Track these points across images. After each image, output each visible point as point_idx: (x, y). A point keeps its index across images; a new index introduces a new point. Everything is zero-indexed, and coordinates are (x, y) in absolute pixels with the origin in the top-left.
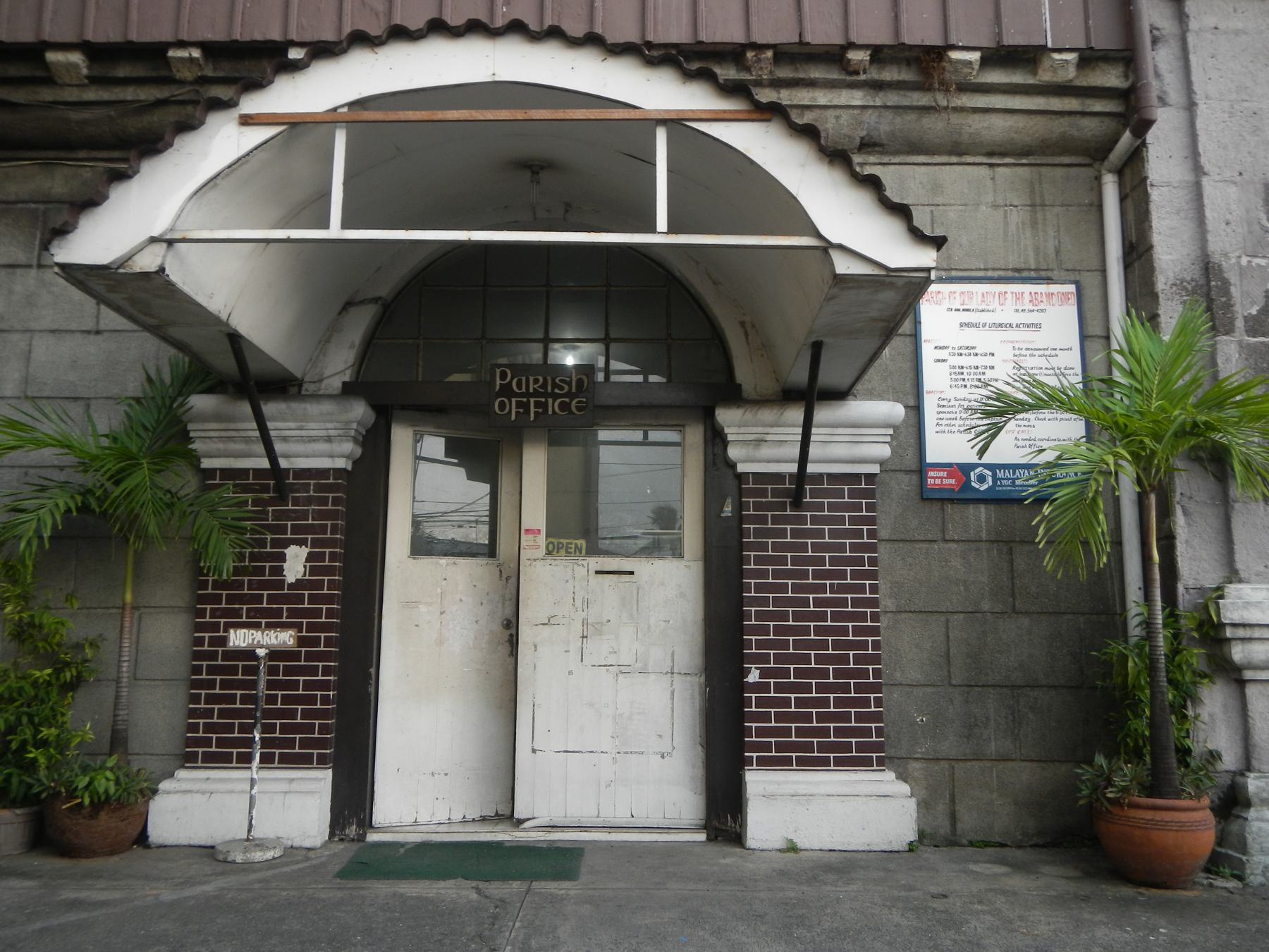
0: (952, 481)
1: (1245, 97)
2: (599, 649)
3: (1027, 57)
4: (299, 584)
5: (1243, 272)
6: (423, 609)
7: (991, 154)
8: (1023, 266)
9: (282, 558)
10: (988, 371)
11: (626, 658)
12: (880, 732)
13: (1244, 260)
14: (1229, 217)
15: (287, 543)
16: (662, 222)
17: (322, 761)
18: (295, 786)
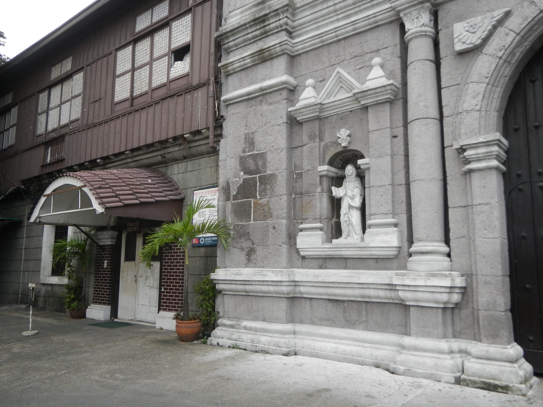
0: (197, 242)
1: (238, 132)
2: (148, 282)
3: (199, 132)
4: (106, 268)
5: (233, 182)
6: (125, 273)
7: (208, 154)
8: (214, 183)
9: (104, 263)
10: (205, 213)
11: (151, 285)
12: (182, 304)
13: (234, 180)
14: (231, 168)
15: (104, 260)
16: (80, 208)
17: (108, 304)
18: (102, 309)
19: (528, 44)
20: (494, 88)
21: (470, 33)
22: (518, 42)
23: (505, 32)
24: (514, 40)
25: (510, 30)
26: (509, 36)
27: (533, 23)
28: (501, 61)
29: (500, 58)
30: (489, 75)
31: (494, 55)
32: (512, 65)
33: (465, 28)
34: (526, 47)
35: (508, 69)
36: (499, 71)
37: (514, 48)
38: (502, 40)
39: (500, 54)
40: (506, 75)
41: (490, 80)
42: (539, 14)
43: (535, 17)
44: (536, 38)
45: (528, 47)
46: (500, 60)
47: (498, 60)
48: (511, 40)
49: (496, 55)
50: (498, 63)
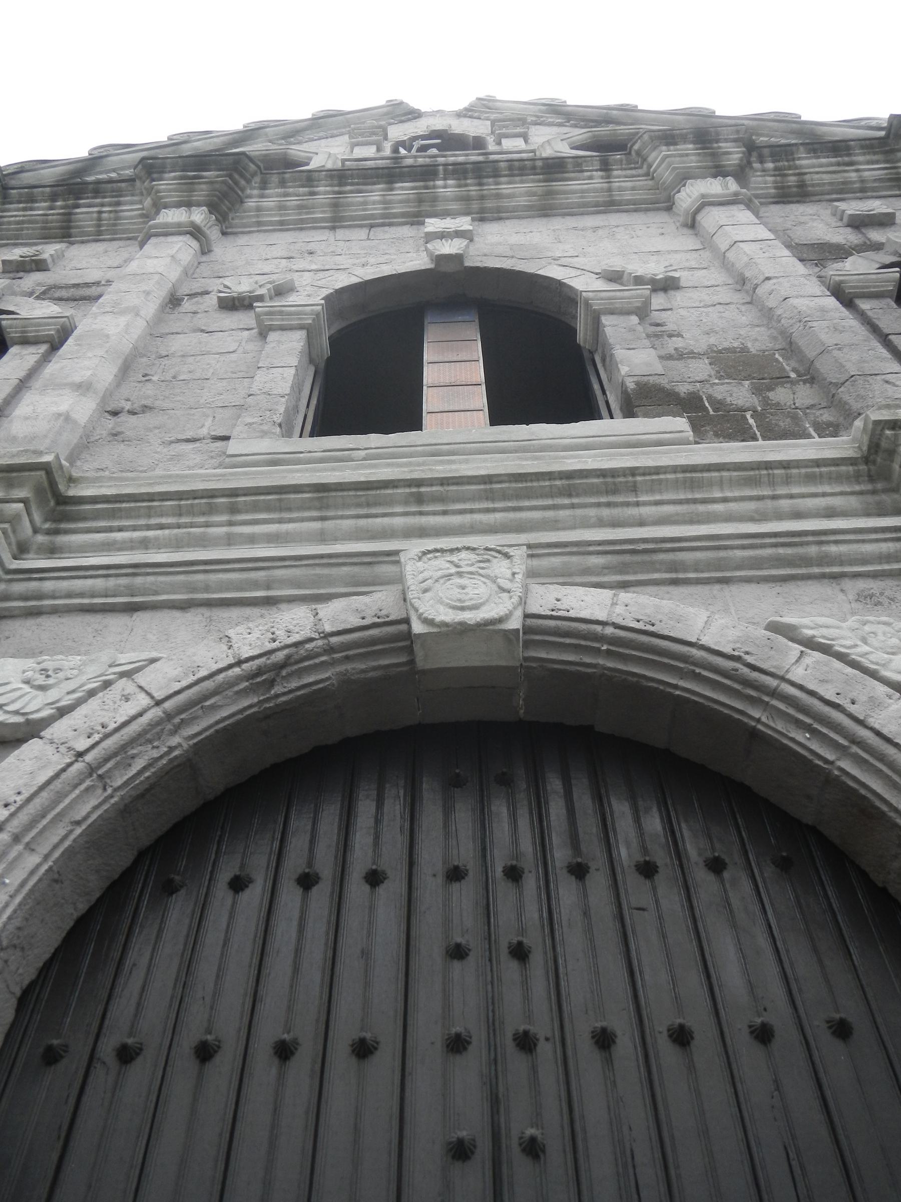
19: (180, 745)
20: (20, 847)
21: (33, 687)
22: (153, 725)
23: (123, 690)
24: (140, 714)
25: (141, 687)
26: (129, 703)
27: (209, 685)
28: (79, 766)
29: (80, 755)
30: (19, 799)
31: (63, 743)
32: (109, 791)
33: (24, 672)
34: (171, 749)
35: (94, 802)
36: (60, 796)
37: (133, 741)
38: (106, 707)
39: (82, 744)
40: (78, 817)
41: (13, 815)
42: (230, 666)
43: (220, 671)
44: (208, 733)
45: (176, 753)
46: (76, 761)
47: (68, 761)
48: (133, 712)
49: (71, 744)
50: (64, 770)
